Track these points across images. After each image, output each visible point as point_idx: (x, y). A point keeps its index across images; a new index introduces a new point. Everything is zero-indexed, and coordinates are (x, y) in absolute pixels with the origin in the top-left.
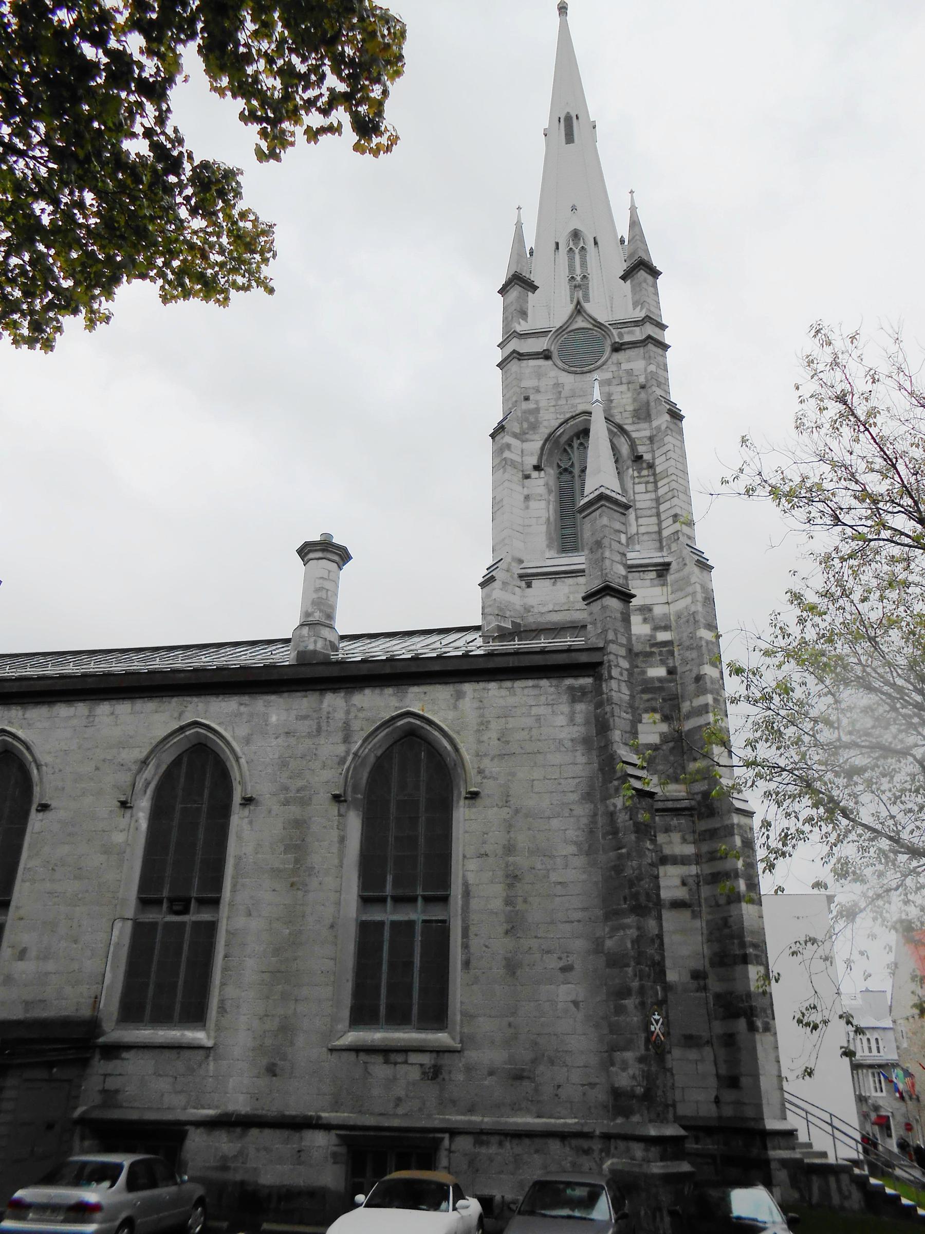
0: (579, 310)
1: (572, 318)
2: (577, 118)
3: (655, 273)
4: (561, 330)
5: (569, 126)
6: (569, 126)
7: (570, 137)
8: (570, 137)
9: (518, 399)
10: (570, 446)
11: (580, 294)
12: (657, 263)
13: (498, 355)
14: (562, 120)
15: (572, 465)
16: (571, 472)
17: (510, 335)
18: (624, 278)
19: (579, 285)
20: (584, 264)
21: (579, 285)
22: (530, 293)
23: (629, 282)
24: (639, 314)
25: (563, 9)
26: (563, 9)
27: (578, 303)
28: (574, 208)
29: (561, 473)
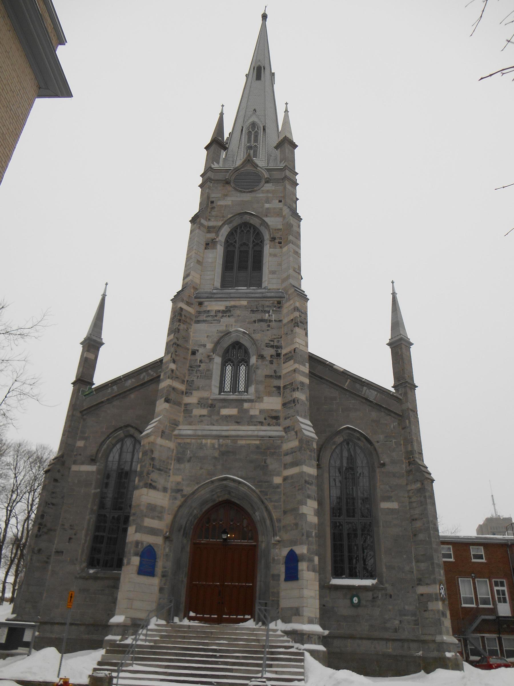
0: (248, 161)
1: (244, 164)
2: (264, 68)
3: (295, 146)
4: (237, 169)
5: (260, 72)
6: (260, 72)
7: (259, 77)
8: (259, 77)
9: (207, 204)
10: (236, 231)
11: (252, 152)
12: (295, 140)
13: (200, 180)
14: (255, 69)
15: (235, 242)
16: (234, 246)
17: (208, 169)
18: (277, 147)
19: (252, 149)
20: (256, 140)
21: (252, 149)
22: (222, 151)
23: (279, 150)
24: (282, 165)
25: (264, 17)
26: (264, 17)
27: (249, 155)
28: (255, 110)
29: (228, 246)
